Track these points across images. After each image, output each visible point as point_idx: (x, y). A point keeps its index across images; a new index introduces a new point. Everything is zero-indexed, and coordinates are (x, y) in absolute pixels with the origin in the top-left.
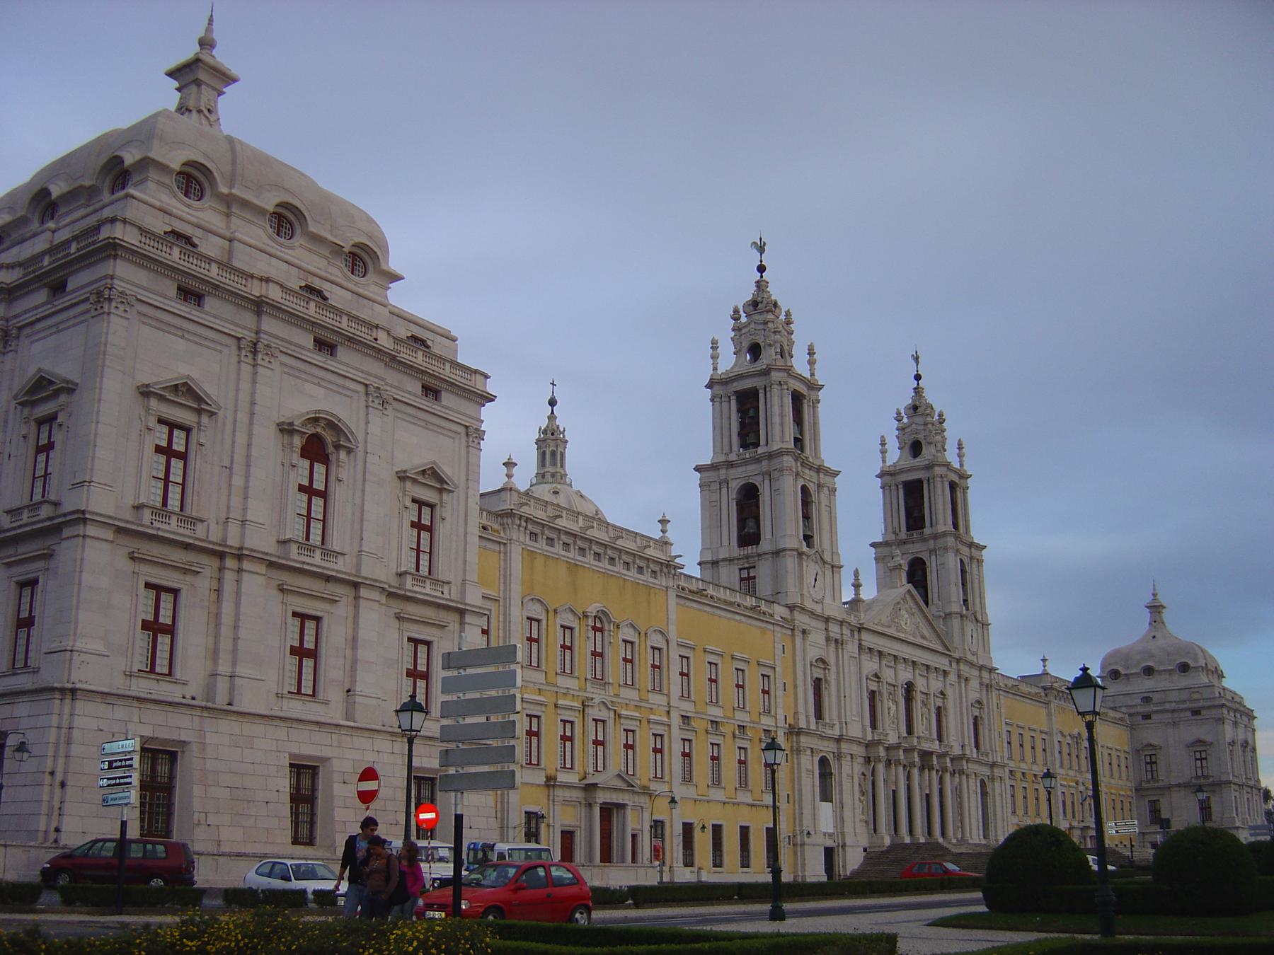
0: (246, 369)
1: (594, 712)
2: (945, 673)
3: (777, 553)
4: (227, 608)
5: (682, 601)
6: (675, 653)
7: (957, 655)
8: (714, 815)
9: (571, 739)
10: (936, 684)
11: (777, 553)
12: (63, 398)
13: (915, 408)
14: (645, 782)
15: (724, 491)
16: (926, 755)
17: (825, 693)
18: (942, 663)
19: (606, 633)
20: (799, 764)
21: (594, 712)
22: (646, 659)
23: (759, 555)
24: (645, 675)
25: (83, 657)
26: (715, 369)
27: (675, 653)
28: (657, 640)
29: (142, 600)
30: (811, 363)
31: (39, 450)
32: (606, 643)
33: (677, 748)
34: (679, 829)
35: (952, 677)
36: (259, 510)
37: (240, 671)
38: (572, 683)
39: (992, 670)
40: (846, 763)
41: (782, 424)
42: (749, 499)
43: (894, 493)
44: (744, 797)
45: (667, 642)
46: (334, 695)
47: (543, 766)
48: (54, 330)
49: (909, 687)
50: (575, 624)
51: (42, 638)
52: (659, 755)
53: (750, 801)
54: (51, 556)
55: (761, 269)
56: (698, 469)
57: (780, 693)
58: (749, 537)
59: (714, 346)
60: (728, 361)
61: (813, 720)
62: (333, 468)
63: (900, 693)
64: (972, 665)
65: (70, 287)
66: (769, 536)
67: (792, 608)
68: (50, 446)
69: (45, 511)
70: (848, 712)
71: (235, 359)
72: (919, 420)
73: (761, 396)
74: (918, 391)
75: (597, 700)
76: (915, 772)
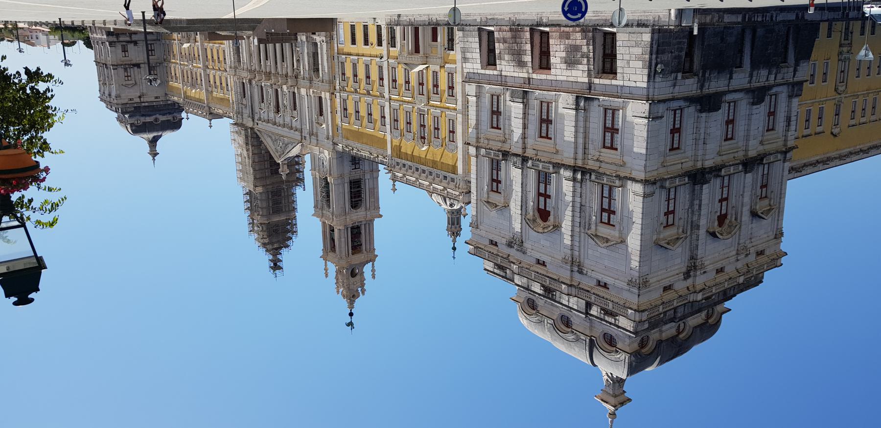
0: (576, 253)
2: (260, 119)
8: (367, 49)
10: (264, 116)
17: (318, 110)
22: (402, 124)
29: (619, 143)
30: (326, 270)
31: (673, 212)
33: (386, 82)
34: (384, 43)
36: (567, 187)
37: (574, 112)
40: (307, 75)
41: (340, 238)
49: (278, 110)
51: (666, 124)
53: (352, 57)
55: (351, 314)
56: (381, 216)
59: (374, 277)
61: (323, 96)
62: (536, 206)
68: (667, 214)
76: (273, 71)
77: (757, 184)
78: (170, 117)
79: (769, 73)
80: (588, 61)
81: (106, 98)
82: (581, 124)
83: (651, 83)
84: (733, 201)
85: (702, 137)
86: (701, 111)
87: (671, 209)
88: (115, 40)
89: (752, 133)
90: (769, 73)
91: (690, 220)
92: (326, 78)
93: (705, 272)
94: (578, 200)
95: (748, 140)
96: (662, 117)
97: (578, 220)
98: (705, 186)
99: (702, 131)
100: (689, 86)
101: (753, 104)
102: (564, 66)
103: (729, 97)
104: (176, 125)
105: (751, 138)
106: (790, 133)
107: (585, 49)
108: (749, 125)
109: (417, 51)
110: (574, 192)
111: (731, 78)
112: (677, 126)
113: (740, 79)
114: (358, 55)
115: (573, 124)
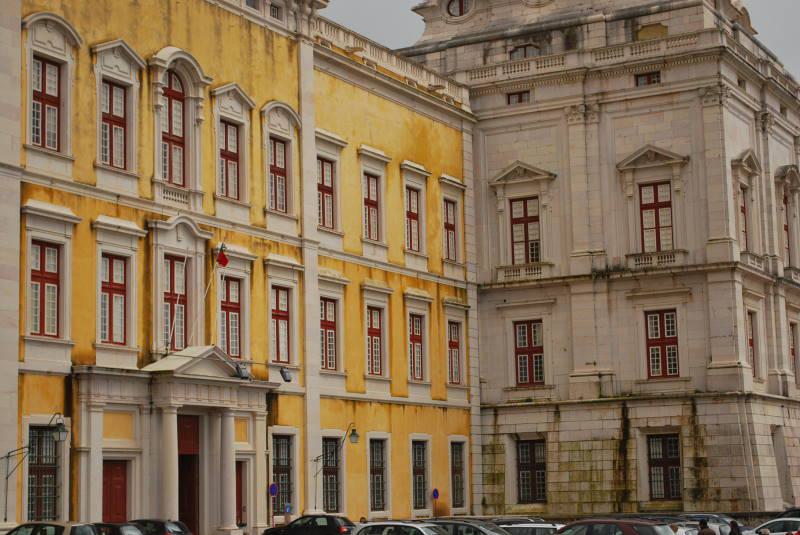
1: (171, 242)
5: (324, 66)
8: (375, 425)
9: (122, 289)
14: (261, 368)
19: (191, 105)
21: (171, 242)
22: (257, 158)
24: (258, 185)
27: (311, 151)
28: (280, 126)
32: (191, 122)
34: (316, 449)
38: (128, 187)
44: (417, 395)
45: (299, 131)
47: (67, 337)
50: (132, 79)
52: (282, 325)
75: (174, 219)
109: (192, 424)
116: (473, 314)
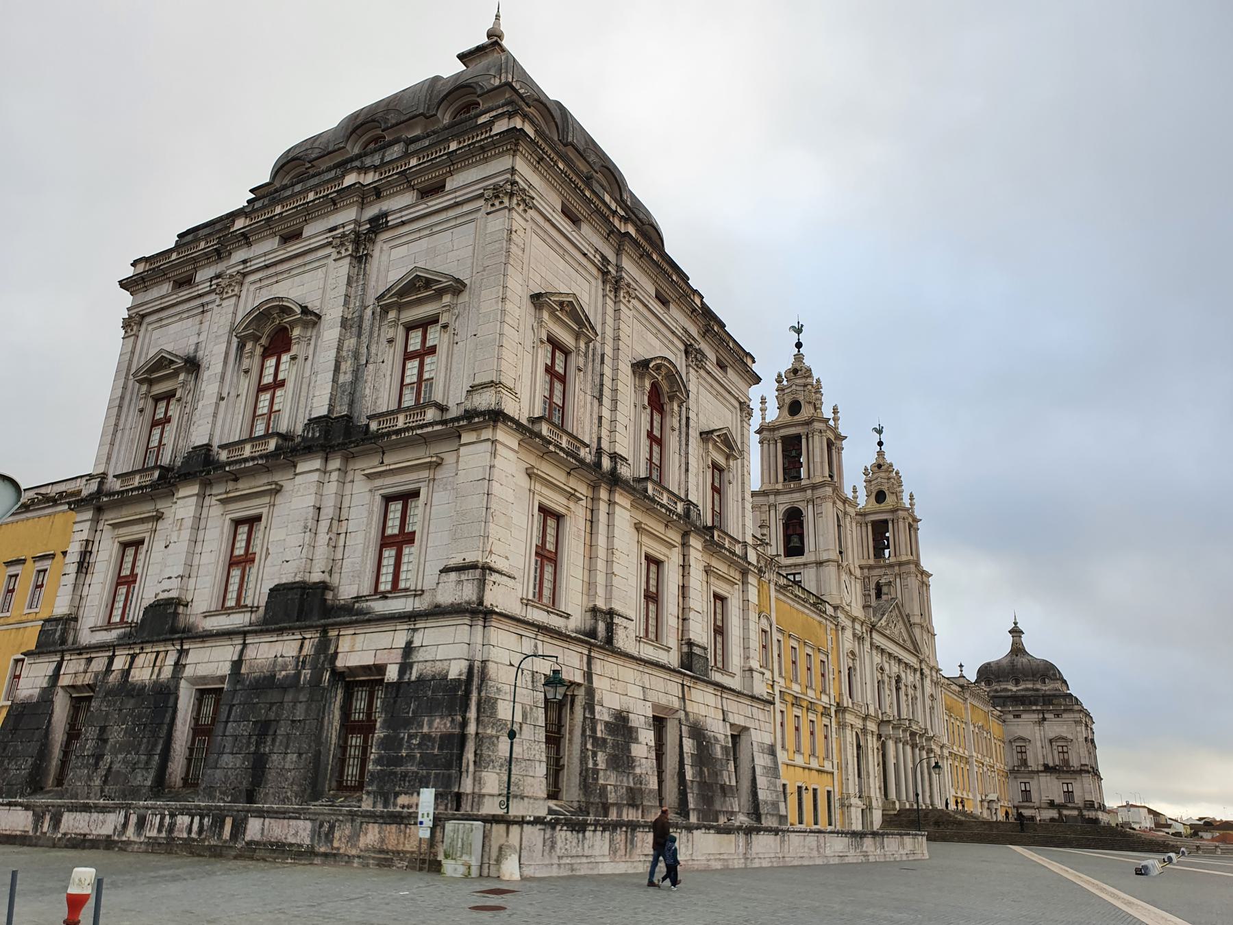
2: (915, 670)
3: (820, 564)
4: (602, 540)
6: (776, 636)
7: (921, 657)
11: (820, 564)
12: (447, 299)
13: (879, 466)
15: (772, 512)
16: (913, 734)
17: (853, 678)
18: (913, 661)
20: (845, 737)
23: (805, 564)
25: (495, 577)
26: (764, 419)
31: (408, 356)
35: (918, 674)
39: (938, 671)
40: (869, 738)
41: (822, 462)
42: (794, 521)
43: (864, 529)
46: (672, 640)
48: (427, 232)
54: (439, 464)
57: (831, 677)
58: (794, 547)
60: (773, 414)
63: (894, 682)
64: (928, 665)
65: (447, 188)
66: (812, 548)
67: (836, 608)
69: (431, 415)
70: (866, 694)
71: (600, 293)
72: (882, 475)
73: (804, 441)
74: (881, 454)
77: (179, 426)
78: (995, 686)
79: (126, 673)
80: (594, 730)
81: (1085, 719)
82: (601, 579)
83: (479, 657)
84: (246, 386)
85: (324, 525)
86: (324, 587)
87: (413, 365)
88: (1085, 812)
89: (186, 534)
90: (126, 673)
91: (365, 339)
92: (848, 731)
93: (331, 230)
94: (606, 413)
95: (198, 519)
96: (446, 570)
97: (607, 371)
98: (323, 411)
99: (323, 538)
100: (358, 649)
101: (177, 602)
102: (636, 721)
103: (239, 620)
104: (987, 673)
105: (188, 523)
106: (84, 536)
107: (601, 757)
108: (191, 553)
110: (612, 431)
111: (237, 665)
112: (389, 553)
113: (212, 661)
114: (810, 769)
115: (616, 581)
116: (833, 719)
